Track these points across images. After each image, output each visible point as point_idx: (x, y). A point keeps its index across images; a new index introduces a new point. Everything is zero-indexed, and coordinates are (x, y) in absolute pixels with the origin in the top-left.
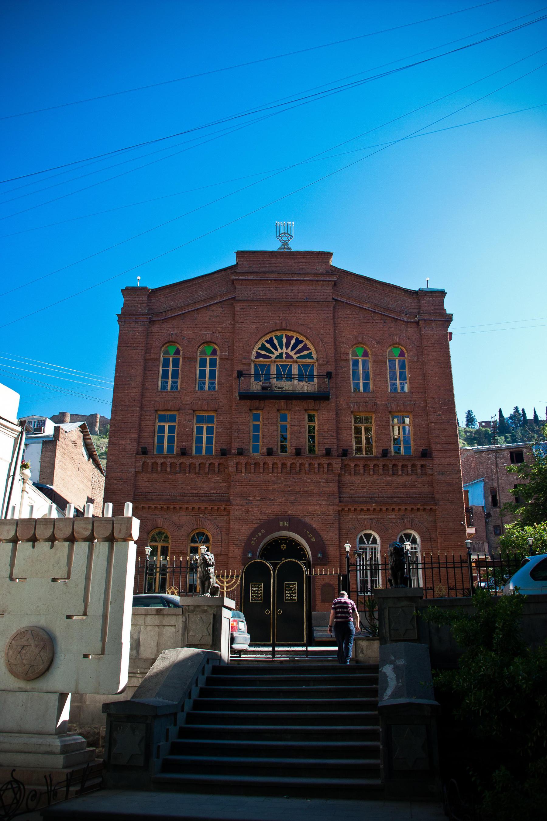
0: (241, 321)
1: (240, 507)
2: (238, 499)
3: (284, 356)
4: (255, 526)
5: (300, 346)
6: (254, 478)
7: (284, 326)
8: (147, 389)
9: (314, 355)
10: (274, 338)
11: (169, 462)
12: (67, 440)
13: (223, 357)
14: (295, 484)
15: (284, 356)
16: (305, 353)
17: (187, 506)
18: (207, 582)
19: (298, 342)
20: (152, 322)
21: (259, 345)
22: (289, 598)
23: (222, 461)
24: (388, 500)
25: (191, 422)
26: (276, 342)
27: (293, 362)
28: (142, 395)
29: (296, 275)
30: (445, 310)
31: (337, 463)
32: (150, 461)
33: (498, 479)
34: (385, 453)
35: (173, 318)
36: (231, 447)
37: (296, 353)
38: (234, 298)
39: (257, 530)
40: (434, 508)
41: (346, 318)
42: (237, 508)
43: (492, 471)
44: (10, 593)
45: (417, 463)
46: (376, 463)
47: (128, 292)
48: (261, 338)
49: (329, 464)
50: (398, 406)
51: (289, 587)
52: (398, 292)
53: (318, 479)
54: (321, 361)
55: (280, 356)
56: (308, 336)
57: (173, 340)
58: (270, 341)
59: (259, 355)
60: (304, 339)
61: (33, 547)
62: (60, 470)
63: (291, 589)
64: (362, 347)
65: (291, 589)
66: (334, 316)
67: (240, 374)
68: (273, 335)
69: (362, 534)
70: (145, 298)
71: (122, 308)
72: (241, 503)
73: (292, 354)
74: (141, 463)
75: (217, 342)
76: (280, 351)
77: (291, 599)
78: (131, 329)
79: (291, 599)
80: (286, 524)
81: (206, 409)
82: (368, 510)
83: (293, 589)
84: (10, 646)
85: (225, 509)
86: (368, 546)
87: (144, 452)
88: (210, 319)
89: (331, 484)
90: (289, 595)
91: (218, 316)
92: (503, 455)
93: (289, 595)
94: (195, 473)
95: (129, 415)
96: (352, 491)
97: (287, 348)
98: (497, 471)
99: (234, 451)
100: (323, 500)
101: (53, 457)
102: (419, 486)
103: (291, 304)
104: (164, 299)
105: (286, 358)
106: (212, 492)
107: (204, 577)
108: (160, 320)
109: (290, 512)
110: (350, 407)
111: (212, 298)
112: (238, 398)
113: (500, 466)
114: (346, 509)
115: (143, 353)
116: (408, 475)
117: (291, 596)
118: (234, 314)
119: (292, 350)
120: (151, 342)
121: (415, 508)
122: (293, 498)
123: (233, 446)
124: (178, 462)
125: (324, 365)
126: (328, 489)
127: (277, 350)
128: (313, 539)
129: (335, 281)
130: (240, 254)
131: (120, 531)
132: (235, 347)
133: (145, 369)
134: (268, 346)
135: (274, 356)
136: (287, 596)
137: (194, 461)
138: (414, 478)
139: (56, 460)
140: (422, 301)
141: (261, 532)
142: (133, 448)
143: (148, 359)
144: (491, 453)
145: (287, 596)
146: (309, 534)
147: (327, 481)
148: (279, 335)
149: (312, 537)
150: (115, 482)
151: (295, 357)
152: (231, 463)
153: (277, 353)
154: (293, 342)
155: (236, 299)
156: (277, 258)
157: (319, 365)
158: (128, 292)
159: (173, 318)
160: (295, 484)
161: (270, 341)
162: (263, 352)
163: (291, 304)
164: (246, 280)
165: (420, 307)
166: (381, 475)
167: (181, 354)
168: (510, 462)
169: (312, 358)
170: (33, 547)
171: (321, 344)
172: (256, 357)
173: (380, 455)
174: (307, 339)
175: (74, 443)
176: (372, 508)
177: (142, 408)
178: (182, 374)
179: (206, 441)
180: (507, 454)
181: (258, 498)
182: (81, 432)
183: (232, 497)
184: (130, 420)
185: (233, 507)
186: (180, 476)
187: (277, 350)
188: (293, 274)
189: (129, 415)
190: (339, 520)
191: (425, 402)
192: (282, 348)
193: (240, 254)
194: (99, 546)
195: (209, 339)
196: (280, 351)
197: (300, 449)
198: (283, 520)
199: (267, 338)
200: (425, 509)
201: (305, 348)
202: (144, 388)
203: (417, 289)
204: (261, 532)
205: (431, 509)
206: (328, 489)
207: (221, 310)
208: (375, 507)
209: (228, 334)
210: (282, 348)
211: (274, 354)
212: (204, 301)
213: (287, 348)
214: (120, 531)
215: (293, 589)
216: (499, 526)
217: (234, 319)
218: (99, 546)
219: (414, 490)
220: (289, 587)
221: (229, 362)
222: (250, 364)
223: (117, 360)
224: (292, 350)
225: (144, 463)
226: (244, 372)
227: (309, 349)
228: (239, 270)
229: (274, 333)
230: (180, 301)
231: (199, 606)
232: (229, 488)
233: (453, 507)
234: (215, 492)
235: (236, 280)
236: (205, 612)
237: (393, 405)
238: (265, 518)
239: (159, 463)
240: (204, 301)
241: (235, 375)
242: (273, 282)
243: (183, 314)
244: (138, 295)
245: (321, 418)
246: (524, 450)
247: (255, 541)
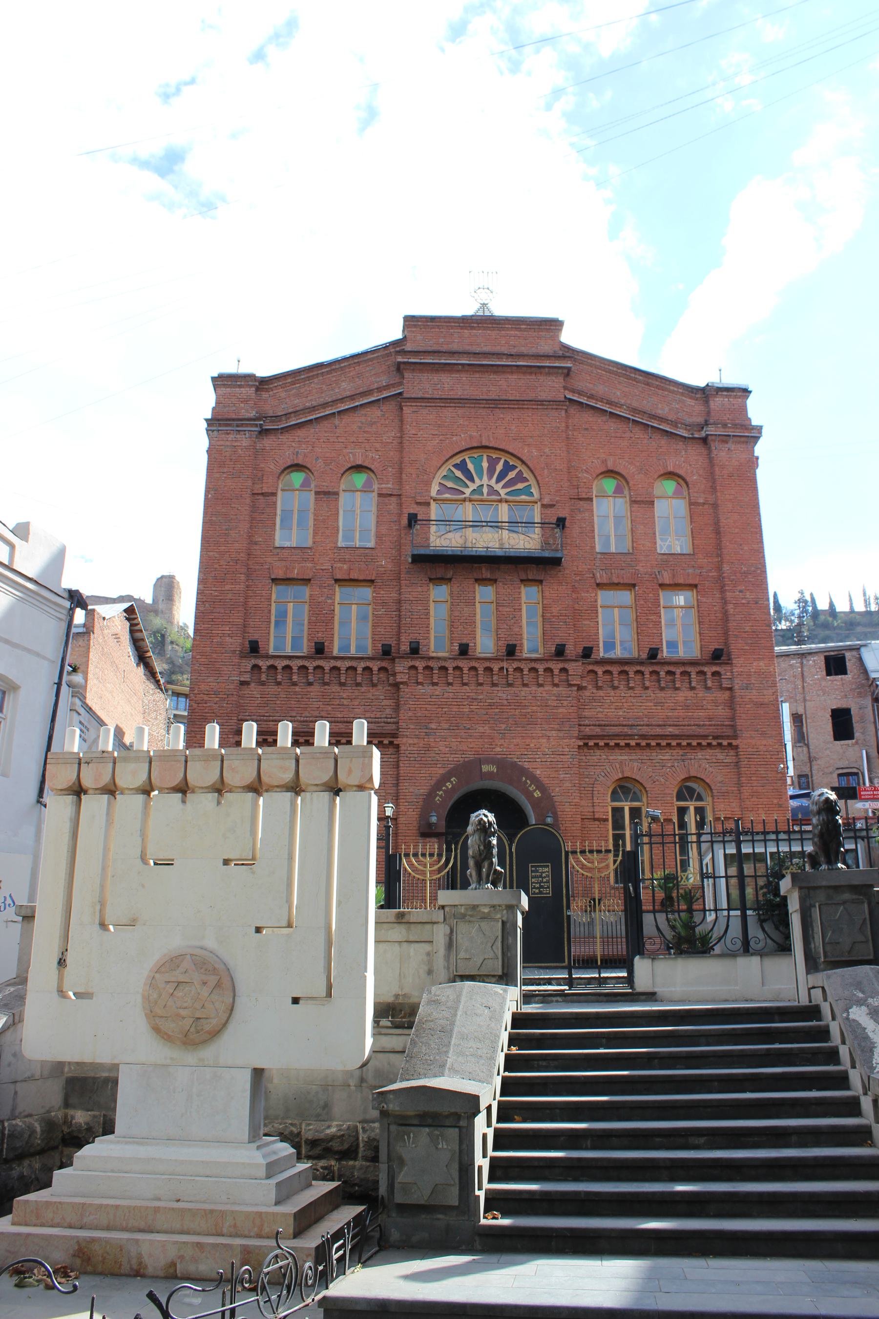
0: (414, 432)
1: (416, 741)
2: (412, 727)
3: (485, 490)
4: (442, 771)
5: (512, 475)
6: (437, 693)
7: (485, 443)
8: (256, 543)
9: (534, 490)
10: (468, 461)
11: (295, 664)
12: (106, 631)
13: (384, 492)
14: (505, 702)
15: (485, 490)
16: (520, 486)
18: (486, 864)
19: (508, 468)
20: (264, 432)
21: (443, 472)
22: (537, 891)
23: (384, 664)
24: (659, 731)
25: (331, 598)
26: (470, 466)
27: (500, 501)
29: (505, 357)
30: (750, 420)
31: (576, 668)
32: (263, 664)
33: (805, 700)
34: (653, 654)
36: (399, 639)
37: (503, 487)
38: (400, 394)
39: (445, 778)
40: (734, 743)
41: (586, 429)
42: (411, 741)
43: (796, 688)
44: (143, 886)
45: (706, 669)
46: (638, 668)
47: (222, 382)
48: (447, 460)
49: (564, 670)
50: (672, 576)
52: (672, 388)
53: (544, 695)
54: (546, 501)
55: (479, 490)
56: (524, 458)
57: (300, 462)
58: (462, 466)
59: (443, 488)
60: (517, 463)
61: (184, 802)
62: (95, 681)
64: (614, 478)
65: (541, 876)
66: (567, 427)
67: (413, 519)
68: (466, 456)
71: (214, 409)
72: (417, 733)
73: (498, 487)
74: (249, 668)
75: (372, 467)
76: (478, 482)
77: (540, 893)
78: (228, 443)
79: (540, 893)
80: (494, 769)
81: (356, 578)
82: (628, 745)
83: (544, 875)
84: (152, 983)
85: (391, 743)
87: (254, 648)
88: (360, 428)
89: (565, 703)
90: (537, 885)
91: (375, 423)
92: (814, 661)
93: (537, 885)
94: (342, 684)
95: (227, 587)
96: (600, 715)
97: (490, 478)
98: (803, 687)
99: (405, 648)
100: (553, 729)
101: (84, 660)
102: (709, 707)
103: (495, 404)
104: (283, 395)
105: (488, 494)
107: (480, 854)
108: (278, 429)
109: (498, 749)
110: (594, 576)
111: (364, 394)
112: (410, 560)
113: (808, 680)
114: (591, 743)
115: (250, 483)
116: (692, 689)
117: (541, 887)
118: (402, 421)
119: (498, 481)
120: (262, 465)
121: (704, 743)
122: (503, 726)
123: (403, 639)
124: (311, 665)
125: (552, 506)
126: (560, 710)
127: (473, 481)
128: (537, 794)
129: (569, 369)
130: (411, 322)
131: (350, 771)
132: (404, 476)
133: (254, 508)
134: (458, 474)
135: (468, 491)
136: (535, 888)
137: (338, 664)
138: (701, 694)
139: (90, 665)
140: (712, 403)
141: (452, 782)
142: (235, 643)
143: (258, 494)
144: (793, 659)
145: (535, 888)
146: (530, 786)
147: (559, 698)
148: (476, 456)
149: (535, 791)
150: (206, 697)
151: (503, 492)
152: (401, 667)
153: (473, 486)
154: (499, 467)
155: (405, 395)
156: (472, 328)
157: (543, 506)
158: (222, 382)
160: (505, 702)
161: (462, 466)
162: (450, 484)
163: (495, 404)
164: (421, 363)
165: (708, 413)
166: (647, 688)
167: (313, 486)
168: (824, 673)
169: (531, 494)
170: (184, 802)
171: (546, 471)
172: (439, 492)
173: (644, 656)
174: (523, 462)
175: (116, 636)
176: (633, 743)
177: (248, 576)
178: (315, 520)
179: (354, 628)
180: (820, 660)
181: (446, 726)
182: (127, 619)
183: (402, 724)
184: (230, 596)
185: (405, 740)
186: (316, 689)
187: (473, 481)
188: (499, 355)
189: (227, 587)
190: (580, 760)
191: (719, 569)
192: (481, 480)
193: (411, 322)
194: (312, 799)
195: (360, 463)
196: (478, 482)
197: (515, 646)
199: (457, 460)
200: (720, 745)
202: (252, 542)
203: (702, 384)
204: (452, 782)
205: (730, 744)
206: (560, 710)
207: (379, 413)
208: (638, 741)
209: (392, 453)
210: (481, 480)
211: (468, 487)
212: (352, 397)
213: (490, 478)
214: (350, 771)
215: (544, 875)
216: (806, 776)
217: (401, 430)
218: (312, 799)
219: (701, 714)
220: (537, 871)
221: (393, 499)
222: (428, 504)
223: (206, 496)
224: (498, 481)
225: (256, 667)
226: (419, 518)
227: (526, 480)
228: (408, 347)
229: (468, 452)
230: (309, 398)
231: (474, 907)
232: (397, 708)
233: (764, 742)
235: (404, 363)
236: (484, 917)
237: (665, 574)
238: (458, 758)
239: (279, 668)
240: (352, 397)
241: (405, 521)
242: (467, 368)
243: (316, 419)
244: (240, 386)
245: (547, 594)
246: (848, 655)
247: (441, 796)
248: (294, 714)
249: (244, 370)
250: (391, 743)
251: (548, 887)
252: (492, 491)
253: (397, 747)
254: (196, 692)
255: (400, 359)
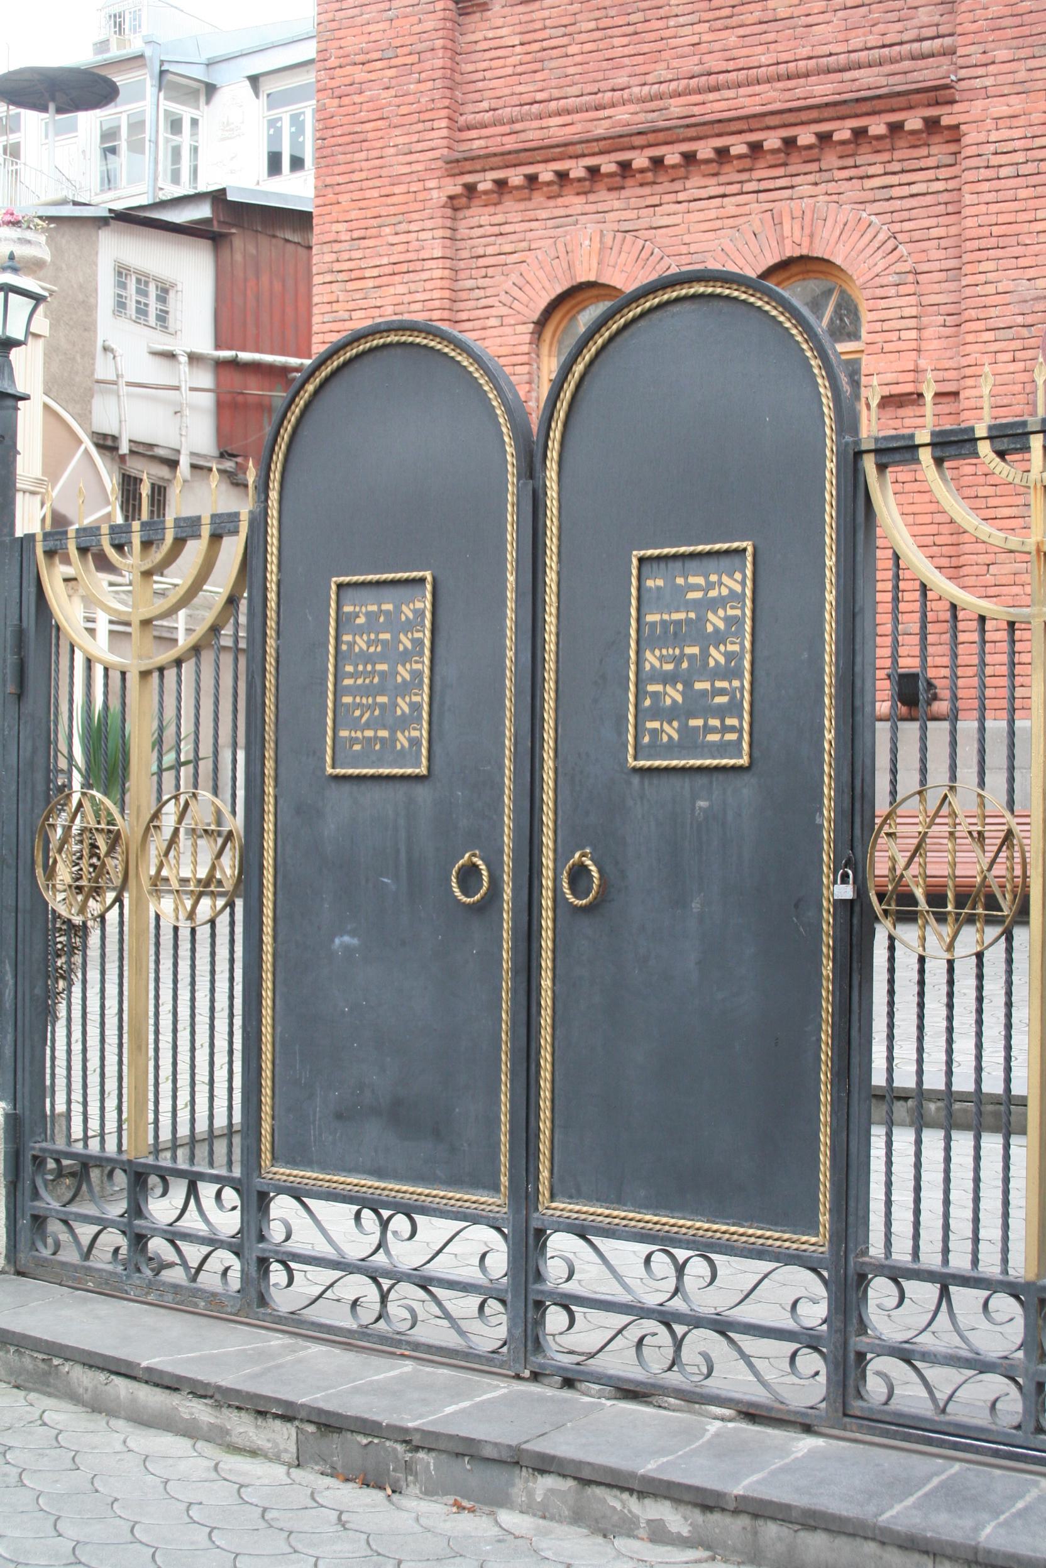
1: (1017, 104)
17: (719, 142)
42: (999, 108)
51: (676, 598)
63: (694, 631)
72: (1022, 75)
85: (932, 124)
90: (674, 694)
93: (674, 694)
106: (856, 43)
145: (657, 713)
215: (715, 621)
234: (873, 40)
248: (622, 81)
250: (932, 124)
251: (734, 708)
253: (955, 134)
254: (333, 62)
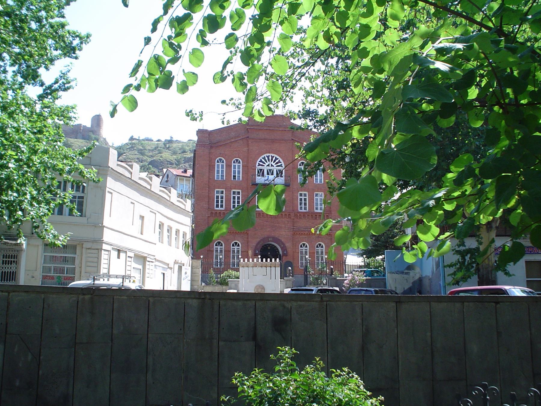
5: (277, 161)
20: (211, 147)
28: (209, 182)
35: (221, 146)
55: (268, 165)
69: (301, 243)
70: (207, 135)
73: (273, 164)
86: (304, 248)
111: (238, 137)
153: (267, 164)
159: (221, 146)
162: (261, 163)
163: (273, 141)
177: (209, 188)
196: (268, 163)
198: (270, 237)
201: (279, 162)
249: (205, 128)
252: (272, 166)
255: (248, 127)
